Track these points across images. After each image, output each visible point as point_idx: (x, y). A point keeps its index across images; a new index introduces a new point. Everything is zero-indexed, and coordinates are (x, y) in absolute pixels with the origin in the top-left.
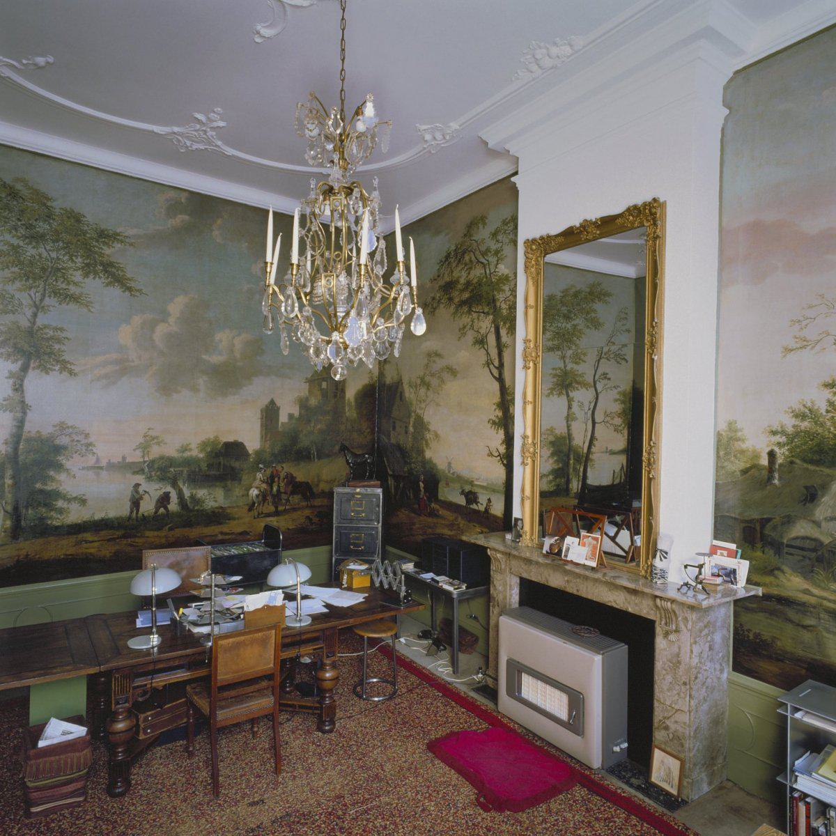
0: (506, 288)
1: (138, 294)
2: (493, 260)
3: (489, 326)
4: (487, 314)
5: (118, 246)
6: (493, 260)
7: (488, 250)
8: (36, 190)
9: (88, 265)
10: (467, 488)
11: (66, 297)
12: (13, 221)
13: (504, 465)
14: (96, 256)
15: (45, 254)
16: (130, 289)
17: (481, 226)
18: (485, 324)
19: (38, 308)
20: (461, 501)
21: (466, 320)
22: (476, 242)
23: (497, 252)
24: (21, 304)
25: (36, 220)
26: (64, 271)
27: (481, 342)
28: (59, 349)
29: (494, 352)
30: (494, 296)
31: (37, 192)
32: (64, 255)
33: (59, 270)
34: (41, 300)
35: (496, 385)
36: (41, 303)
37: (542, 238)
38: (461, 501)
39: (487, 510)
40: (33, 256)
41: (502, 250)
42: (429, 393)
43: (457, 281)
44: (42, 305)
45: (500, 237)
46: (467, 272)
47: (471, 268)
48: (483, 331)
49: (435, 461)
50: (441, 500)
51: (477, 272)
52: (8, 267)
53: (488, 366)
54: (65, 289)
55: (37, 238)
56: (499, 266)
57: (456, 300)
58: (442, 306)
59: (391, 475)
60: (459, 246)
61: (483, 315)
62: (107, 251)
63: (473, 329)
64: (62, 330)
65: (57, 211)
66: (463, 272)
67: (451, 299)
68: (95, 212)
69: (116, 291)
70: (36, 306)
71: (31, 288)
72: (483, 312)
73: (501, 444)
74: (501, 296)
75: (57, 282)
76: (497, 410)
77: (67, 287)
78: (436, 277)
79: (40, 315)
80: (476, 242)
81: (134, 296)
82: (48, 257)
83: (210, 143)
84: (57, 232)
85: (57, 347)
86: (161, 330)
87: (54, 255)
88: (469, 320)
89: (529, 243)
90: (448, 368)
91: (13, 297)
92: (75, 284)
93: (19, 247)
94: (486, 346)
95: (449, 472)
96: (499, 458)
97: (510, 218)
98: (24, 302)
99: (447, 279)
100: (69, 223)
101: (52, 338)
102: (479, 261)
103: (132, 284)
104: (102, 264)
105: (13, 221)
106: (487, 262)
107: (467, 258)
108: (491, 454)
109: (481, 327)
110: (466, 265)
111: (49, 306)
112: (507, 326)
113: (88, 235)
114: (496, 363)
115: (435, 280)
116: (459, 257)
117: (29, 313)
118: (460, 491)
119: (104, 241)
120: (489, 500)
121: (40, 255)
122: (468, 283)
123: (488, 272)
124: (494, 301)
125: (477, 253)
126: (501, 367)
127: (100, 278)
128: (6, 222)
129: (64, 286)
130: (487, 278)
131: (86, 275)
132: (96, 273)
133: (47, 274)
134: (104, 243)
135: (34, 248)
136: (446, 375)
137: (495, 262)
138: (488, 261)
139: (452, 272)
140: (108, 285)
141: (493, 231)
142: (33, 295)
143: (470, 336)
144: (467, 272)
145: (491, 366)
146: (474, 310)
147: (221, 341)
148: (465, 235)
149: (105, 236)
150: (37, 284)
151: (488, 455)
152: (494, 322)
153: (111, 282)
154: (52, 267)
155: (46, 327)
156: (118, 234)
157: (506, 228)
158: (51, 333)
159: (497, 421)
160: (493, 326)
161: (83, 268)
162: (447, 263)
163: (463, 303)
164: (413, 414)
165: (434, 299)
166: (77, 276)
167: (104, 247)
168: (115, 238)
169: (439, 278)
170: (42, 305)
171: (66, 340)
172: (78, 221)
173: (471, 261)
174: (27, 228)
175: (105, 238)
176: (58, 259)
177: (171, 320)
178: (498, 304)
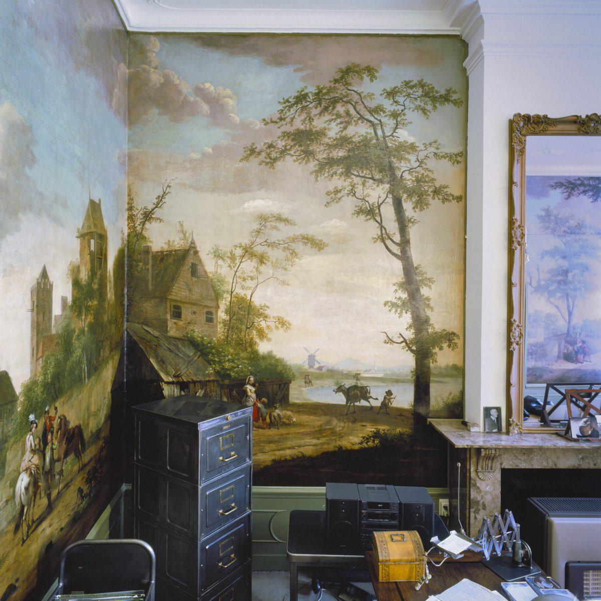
0: (412, 158)
2: (390, 123)
3: (384, 196)
4: (381, 181)
7: (378, 110)
10: (348, 383)
13: (412, 351)
20: (340, 399)
21: (338, 182)
22: (359, 94)
23: (395, 115)
27: (371, 212)
29: (392, 227)
35: (398, 265)
38: (340, 399)
39: (384, 405)
42: (263, 268)
46: (342, 126)
47: (348, 123)
48: (373, 199)
49: (278, 354)
50: (294, 405)
53: (383, 241)
57: (322, 156)
59: (168, 383)
60: (324, 91)
61: (371, 181)
66: (333, 125)
72: (372, 178)
73: (407, 329)
74: (403, 164)
76: (400, 292)
78: (275, 119)
80: (359, 94)
90: (303, 238)
94: (378, 219)
95: (311, 367)
96: (404, 344)
97: (415, 81)
99: (299, 124)
102: (362, 118)
107: (340, 108)
108: (390, 341)
109: (369, 196)
110: (338, 116)
114: (397, 238)
116: (324, 104)
118: (336, 387)
120: (389, 393)
123: (380, 133)
125: (360, 107)
126: (405, 243)
130: (378, 139)
136: (299, 247)
138: (380, 121)
139: (311, 119)
141: (389, 90)
143: (349, 204)
145: (388, 242)
151: (385, 342)
152: (391, 191)
159: (400, 303)
160: (390, 196)
163: (331, 162)
164: (227, 296)
165: (270, 146)
169: (283, 122)
173: (348, 113)
178: (399, 174)
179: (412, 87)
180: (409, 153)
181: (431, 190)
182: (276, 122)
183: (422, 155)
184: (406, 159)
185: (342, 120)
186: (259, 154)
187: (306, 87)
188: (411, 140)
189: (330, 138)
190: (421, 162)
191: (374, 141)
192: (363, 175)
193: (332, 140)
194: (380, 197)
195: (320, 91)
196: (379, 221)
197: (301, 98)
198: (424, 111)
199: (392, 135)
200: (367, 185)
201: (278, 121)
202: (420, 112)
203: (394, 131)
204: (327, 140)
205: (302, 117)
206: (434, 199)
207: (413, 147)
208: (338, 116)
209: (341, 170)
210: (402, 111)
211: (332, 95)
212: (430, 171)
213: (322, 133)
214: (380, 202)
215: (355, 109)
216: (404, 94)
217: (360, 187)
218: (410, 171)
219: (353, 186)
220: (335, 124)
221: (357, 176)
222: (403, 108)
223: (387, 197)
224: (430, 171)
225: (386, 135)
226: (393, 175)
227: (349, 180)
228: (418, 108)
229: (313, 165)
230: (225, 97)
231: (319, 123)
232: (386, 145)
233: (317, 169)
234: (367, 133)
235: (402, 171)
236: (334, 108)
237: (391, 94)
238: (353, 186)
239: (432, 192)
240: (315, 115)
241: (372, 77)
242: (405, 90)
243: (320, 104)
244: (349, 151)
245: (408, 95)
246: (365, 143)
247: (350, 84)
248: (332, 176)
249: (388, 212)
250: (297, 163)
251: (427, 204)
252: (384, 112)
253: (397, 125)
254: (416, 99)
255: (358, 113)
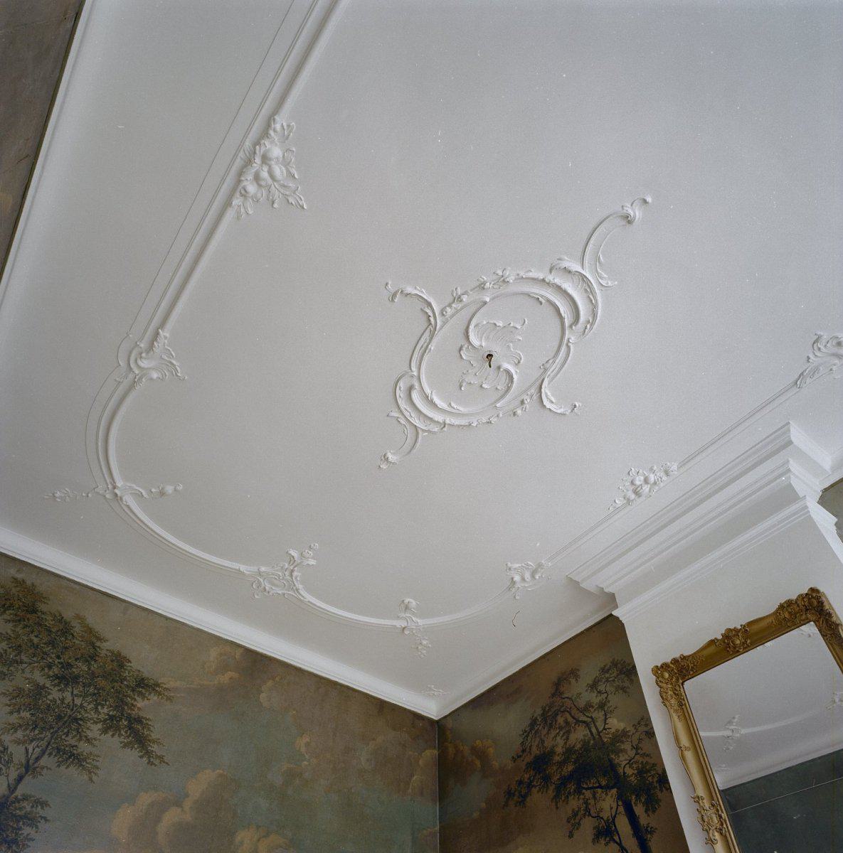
0: (627, 746)
1: (157, 762)
2: (599, 715)
3: (614, 806)
4: (607, 788)
5: (154, 698)
6: (599, 715)
7: (589, 706)
8: (91, 629)
9: (112, 718)
11: (70, 757)
12: (51, 658)
14: (126, 708)
15: (69, 699)
16: (148, 754)
17: (573, 681)
18: (608, 803)
19: (29, 768)
21: (574, 803)
23: (602, 706)
24: (10, 761)
25: (76, 660)
26: (81, 722)
28: (28, 835)
30: (611, 761)
31: (90, 630)
32: (89, 704)
33: (76, 720)
34: (38, 759)
36: (34, 764)
37: (675, 661)
40: (54, 701)
41: (609, 702)
43: (552, 752)
44: (36, 765)
45: (601, 687)
46: (565, 737)
47: (569, 732)
51: (579, 735)
52: (18, 711)
54: (73, 747)
55: (64, 680)
56: (609, 721)
57: (555, 778)
58: (534, 790)
61: (599, 790)
62: (140, 703)
63: (590, 815)
64: (44, 804)
65: (103, 653)
66: (558, 738)
67: (547, 779)
68: (143, 659)
69: (133, 755)
70: (27, 767)
71: (32, 741)
72: (600, 787)
74: (622, 758)
75: (67, 736)
77: (76, 744)
79: (27, 779)
81: (152, 764)
82: (71, 703)
83: (292, 587)
84: (93, 675)
85: (27, 830)
86: (171, 817)
87: (78, 701)
88: (581, 801)
89: (659, 671)
91: (6, 749)
92: (88, 740)
93: (44, 687)
94: (616, 838)
98: (16, 760)
99: (535, 751)
100: (111, 667)
101: (25, 817)
102: (578, 722)
103: (154, 748)
104: (129, 718)
105: (51, 658)
106: (589, 720)
107: (560, 720)
109: (601, 810)
111: (42, 768)
112: (643, 800)
113: (125, 683)
115: (519, 757)
116: (549, 722)
117: (14, 774)
119: (140, 692)
121: (62, 700)
122: (569, 751)
123: (594, 730)
124: (613, 766)
125: (574, 711)
127: (120, 735)
128: (43, 658)
129: (73, 742)
130: (594, 739)
131: (105, 731)
132: (118, 729)
133: (60, 724)
134: (140, 694)
135: (60, 690)
137: (603, 718)
138: (591, 718)
139: (543, 742)
140: (125, 745)
141: (591, 683)
142: (30, 751)
143: (588, 825)
144: (565, 737)
146: (585, 786)
147: (242, 843)
148: (553, 695)
149: (144, 685)
150: (43, 736)
152: (620, 797)
153: (131, 742)
154: (70, 716)
155: (25, 798)
156: (158, 685)
157: (607, 675)
158: (28, 809)
160: (620, 803)
161: (105, 720)
162: (533, 732)
163: (564, 781)
165: (520, 782)
166: (94, 730)
167: (137, 698)
168: (154, 689)
169: (525, 754)
170: (36, 765)
171: (43, 821)
172: (121, 666)
173: (567, 722)
174: (63, 667)
175: (142, 687)
176: (82, 706)
177: (188, 804)
178: (621, 771)
179: (607, 671)
180: (623, 742)
181: (656, 779)
182: (521, 756)
183: (635, 739)
184: (622, 751)
185: (564, 731)
186: (514, 795)
187: (535, 712)
188: (621, 726)
189: (559, 755)
190: (637, 748)
191: (592, 742)
192: (591, 785)
193: (560, 755)
194: (611, 808)
195: (544, 709)
196: (618, 840)
197: (534, 722)
198: (624, 689)
199: (604, 729)
200: (598, 795)
201: (521, 754)
202: (621, 691)
203: (605, 724)
204: (557, 758)
205: (537, 743)
206: (662, 791)
207: (624, 733)
208: (561, 728)
209: (573, 787)
210: (606, 698)
211: (553, 710)
212: (648, 755)
213: (552, 752)
214: (613, 814)
215: (570, 714)
216: (604, 681)
217: (592, 802)
218: (630, 763)
219: (586, 803)
220: (559, 737)
221: (587, 789)
222: (606, 695)
223: (618, 805)
224: (648, 755)
225: (600, 730)
226: (617, 776)
227: (582, 797)
228: (617, 688)
229: (551, 792)
230: (488, 748)
231: (548, 743)
232: (603, 741)
233: (555, 794)
234: (584, 736)
235: (622, 766)
236: (556, 721)
237: (593, 686)
238: (586, 803)
239: (657, 781)
240: (544, 736)
241: (577, 677)
242: (603, 676)
243: (546, 723)
244: (575, 762)
245: (607, 681)
246: (585, 744)
247: (563, 693)
248: (568, 798)
249: (623, 825)
250: (540, 793)
251: (658, 801)
252: (593, 707)
253: (606, 715)
254: (614, 681)
255: (573, 718)
